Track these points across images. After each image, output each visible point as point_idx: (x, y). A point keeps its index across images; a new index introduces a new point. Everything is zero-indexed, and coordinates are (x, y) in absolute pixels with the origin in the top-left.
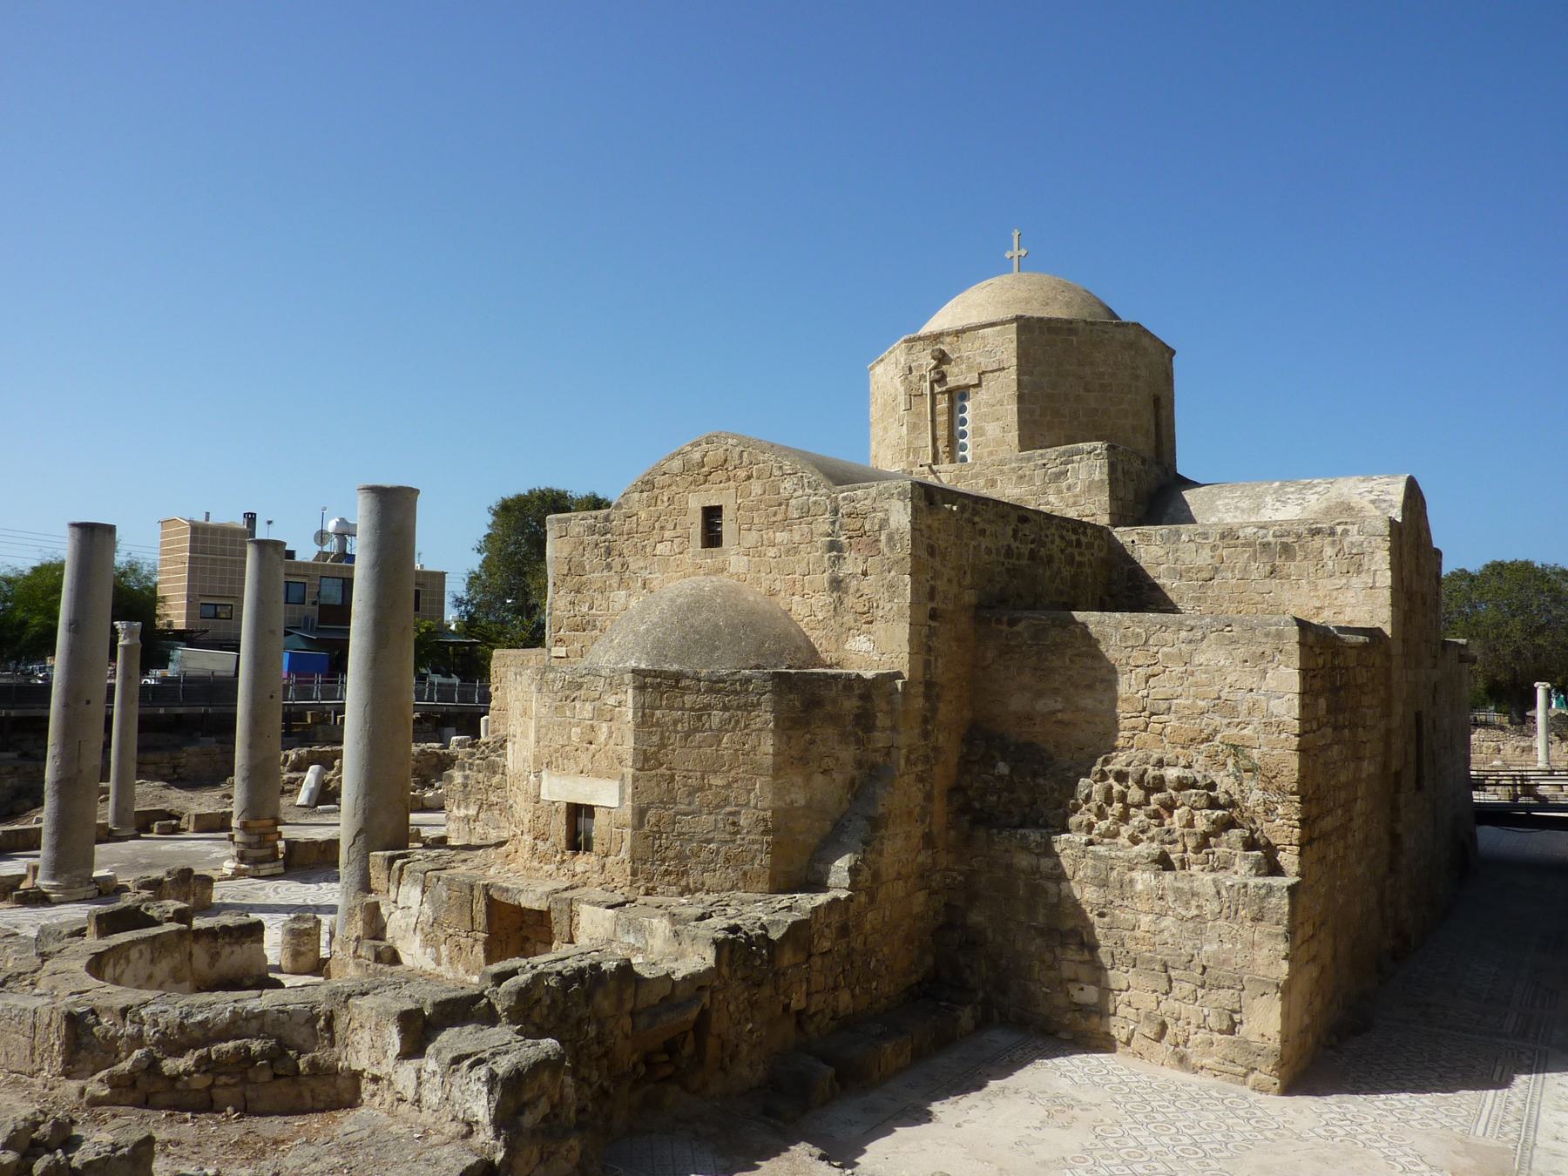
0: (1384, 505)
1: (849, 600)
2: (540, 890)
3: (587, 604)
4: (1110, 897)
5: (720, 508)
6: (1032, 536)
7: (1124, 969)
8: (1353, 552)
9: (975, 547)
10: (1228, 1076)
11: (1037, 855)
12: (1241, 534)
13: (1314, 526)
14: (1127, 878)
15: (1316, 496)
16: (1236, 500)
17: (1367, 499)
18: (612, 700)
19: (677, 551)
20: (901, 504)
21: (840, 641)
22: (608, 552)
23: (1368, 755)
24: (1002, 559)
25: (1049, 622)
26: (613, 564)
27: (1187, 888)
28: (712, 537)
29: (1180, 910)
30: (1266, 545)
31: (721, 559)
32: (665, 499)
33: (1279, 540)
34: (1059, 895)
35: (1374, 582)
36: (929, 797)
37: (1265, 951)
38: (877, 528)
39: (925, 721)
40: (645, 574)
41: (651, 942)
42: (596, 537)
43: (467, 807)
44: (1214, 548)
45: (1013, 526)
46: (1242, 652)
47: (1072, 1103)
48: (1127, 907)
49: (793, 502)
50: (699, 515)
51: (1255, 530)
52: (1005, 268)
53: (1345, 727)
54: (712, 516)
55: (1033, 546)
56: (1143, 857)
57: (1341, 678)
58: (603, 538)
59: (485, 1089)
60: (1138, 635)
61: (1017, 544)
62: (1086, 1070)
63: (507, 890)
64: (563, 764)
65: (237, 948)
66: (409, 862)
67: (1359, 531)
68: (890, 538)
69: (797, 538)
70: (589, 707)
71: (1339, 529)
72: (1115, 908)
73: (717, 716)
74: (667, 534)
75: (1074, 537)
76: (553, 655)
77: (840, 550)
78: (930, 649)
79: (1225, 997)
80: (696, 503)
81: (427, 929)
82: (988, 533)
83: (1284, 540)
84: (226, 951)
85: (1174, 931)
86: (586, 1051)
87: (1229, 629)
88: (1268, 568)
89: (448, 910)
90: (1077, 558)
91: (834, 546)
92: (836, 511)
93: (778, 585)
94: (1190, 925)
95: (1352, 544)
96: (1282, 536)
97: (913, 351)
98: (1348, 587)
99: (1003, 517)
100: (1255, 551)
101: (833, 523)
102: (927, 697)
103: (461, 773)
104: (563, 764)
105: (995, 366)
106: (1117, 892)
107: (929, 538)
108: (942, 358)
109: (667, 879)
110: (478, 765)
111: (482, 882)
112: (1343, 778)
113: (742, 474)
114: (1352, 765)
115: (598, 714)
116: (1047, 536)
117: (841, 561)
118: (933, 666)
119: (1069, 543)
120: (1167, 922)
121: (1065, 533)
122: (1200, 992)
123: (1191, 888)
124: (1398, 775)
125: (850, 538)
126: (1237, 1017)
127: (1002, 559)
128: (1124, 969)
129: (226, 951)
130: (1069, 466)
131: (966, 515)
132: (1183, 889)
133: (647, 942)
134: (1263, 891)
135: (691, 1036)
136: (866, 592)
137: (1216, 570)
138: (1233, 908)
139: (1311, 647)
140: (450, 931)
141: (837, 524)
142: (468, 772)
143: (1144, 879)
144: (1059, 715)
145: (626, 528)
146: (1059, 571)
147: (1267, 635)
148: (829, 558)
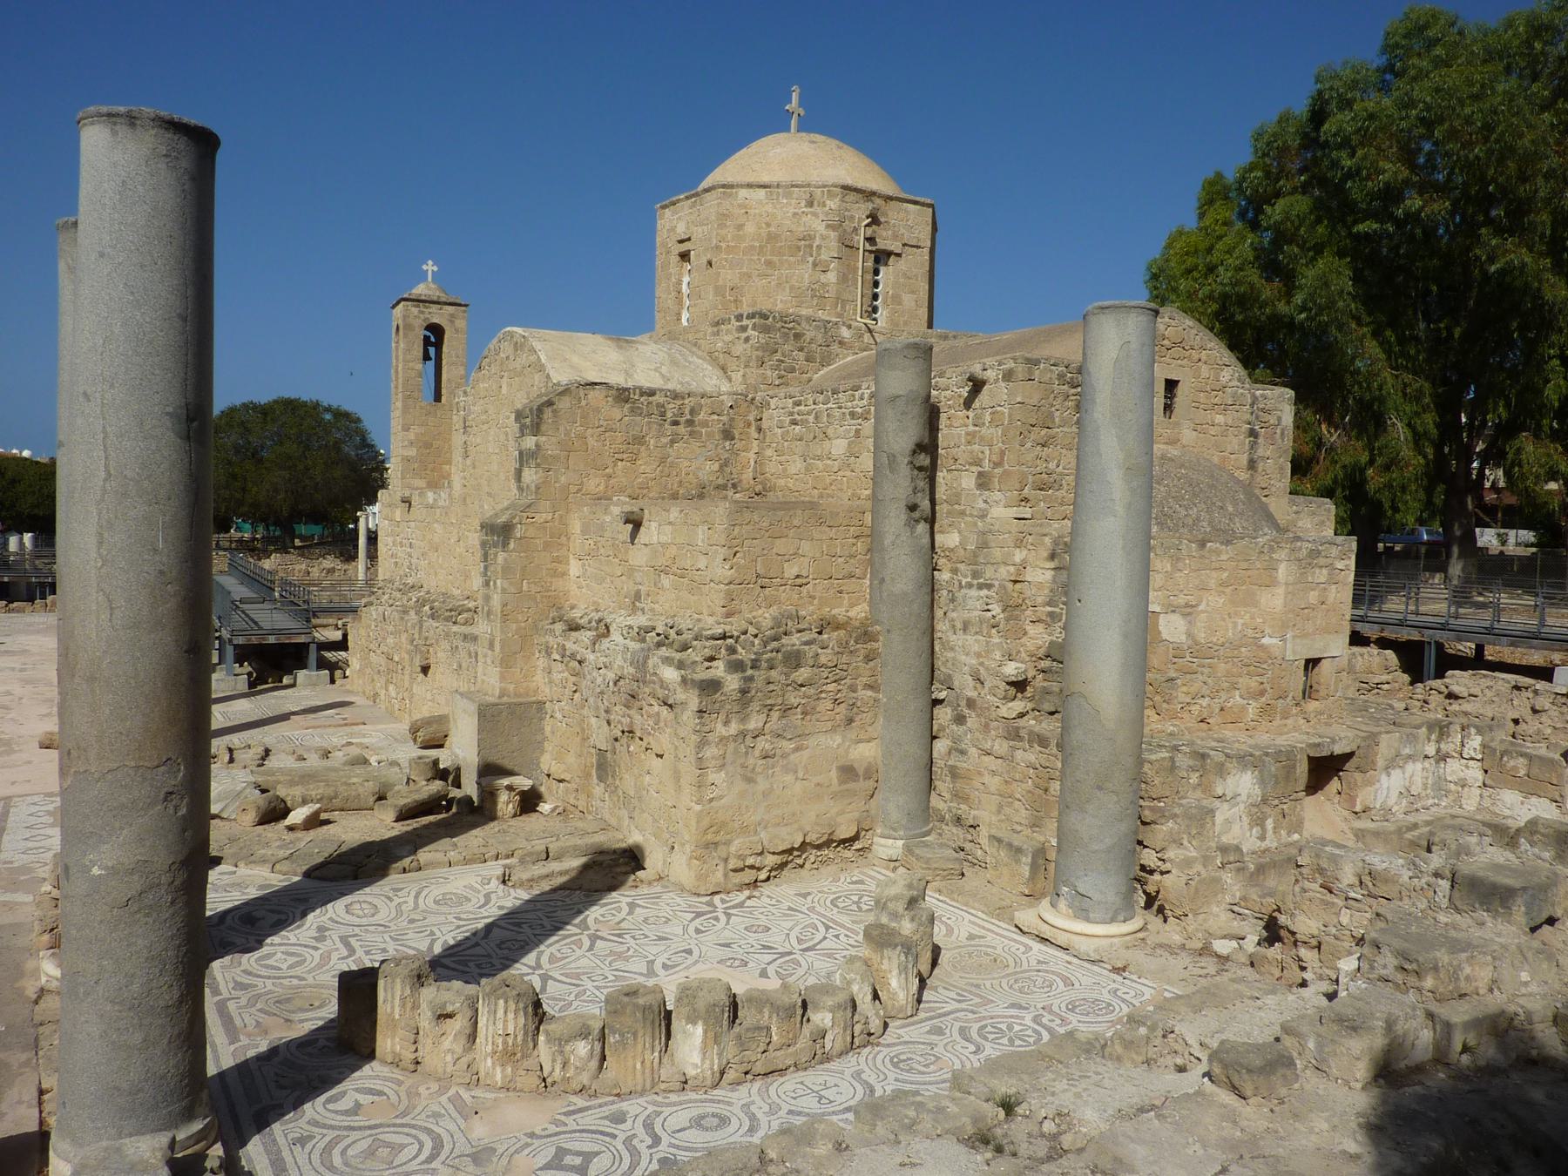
42: (1066, 387)
43: (743, 720)
54: (1171, 385)
70: (1325, 571)
108: (874, 220)
113: (1195, 356)
142: (750, 672)
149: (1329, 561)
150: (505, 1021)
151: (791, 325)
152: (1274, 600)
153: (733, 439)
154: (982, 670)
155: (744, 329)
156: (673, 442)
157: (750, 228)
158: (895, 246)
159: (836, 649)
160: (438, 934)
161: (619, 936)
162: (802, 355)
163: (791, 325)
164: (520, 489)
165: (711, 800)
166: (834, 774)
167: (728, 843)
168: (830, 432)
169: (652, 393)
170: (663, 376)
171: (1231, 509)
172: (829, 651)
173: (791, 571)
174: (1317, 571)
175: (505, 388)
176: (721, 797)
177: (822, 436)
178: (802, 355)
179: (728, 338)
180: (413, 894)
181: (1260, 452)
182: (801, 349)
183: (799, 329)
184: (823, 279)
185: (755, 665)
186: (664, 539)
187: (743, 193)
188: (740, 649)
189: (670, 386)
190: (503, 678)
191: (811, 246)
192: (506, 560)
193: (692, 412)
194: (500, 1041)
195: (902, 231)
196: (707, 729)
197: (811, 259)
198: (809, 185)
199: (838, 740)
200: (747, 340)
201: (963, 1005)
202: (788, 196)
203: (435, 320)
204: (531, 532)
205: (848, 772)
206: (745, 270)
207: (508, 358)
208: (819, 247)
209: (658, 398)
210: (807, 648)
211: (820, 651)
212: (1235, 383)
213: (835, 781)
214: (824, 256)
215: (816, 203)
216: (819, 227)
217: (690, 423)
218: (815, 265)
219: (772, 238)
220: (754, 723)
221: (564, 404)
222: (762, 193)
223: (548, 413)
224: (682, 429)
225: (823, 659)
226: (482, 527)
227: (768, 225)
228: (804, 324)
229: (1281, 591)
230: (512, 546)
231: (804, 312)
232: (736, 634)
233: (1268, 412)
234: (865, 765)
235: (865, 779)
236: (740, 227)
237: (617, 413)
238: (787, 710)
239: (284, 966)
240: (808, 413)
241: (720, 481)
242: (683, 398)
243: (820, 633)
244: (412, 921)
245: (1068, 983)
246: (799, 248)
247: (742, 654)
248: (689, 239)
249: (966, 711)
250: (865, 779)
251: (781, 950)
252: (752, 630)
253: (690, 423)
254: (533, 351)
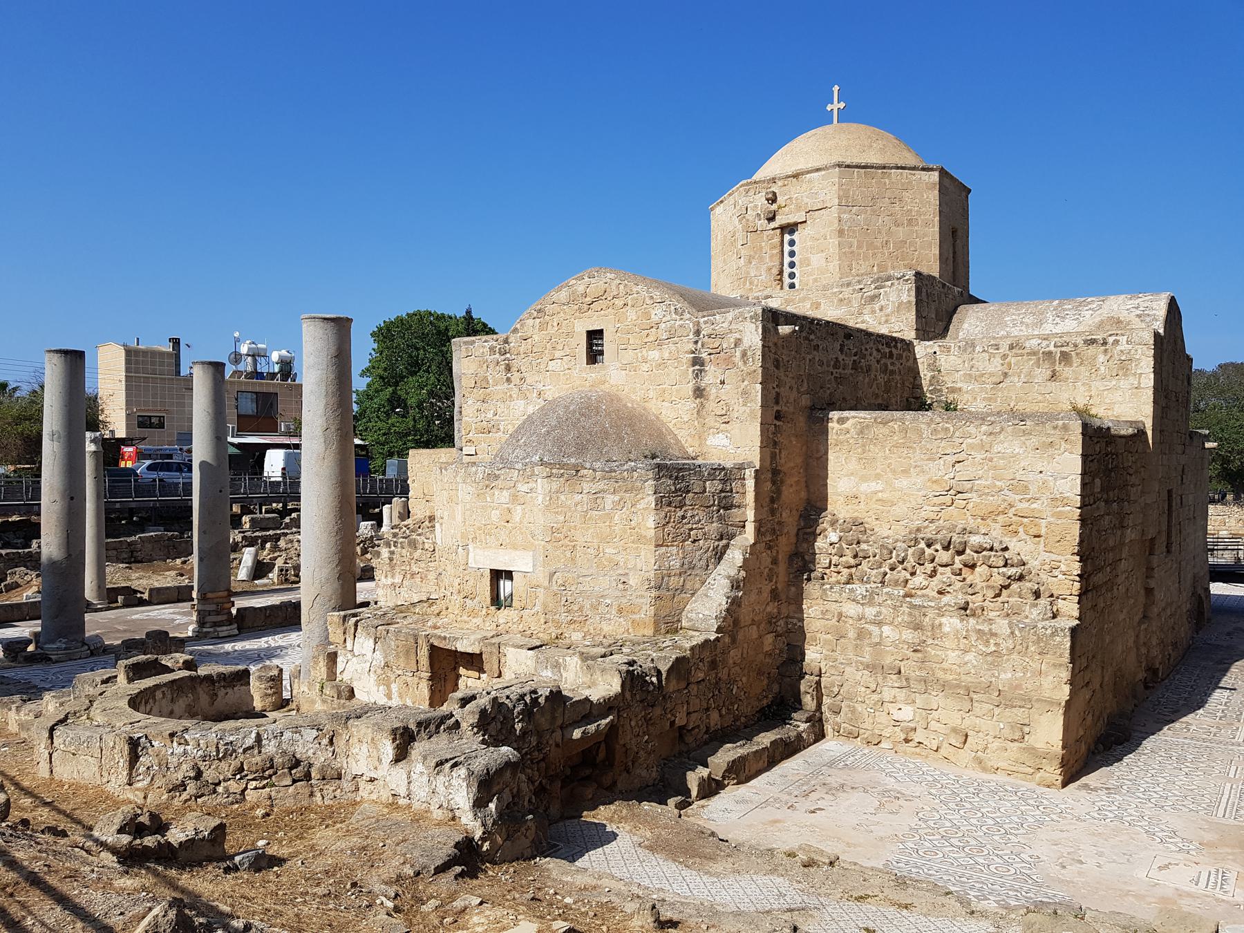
0: (1148, 319)
1: (711, 405)
2: (472, 638)
3: (492, 412)
4: (924, 638)
5: (601, 332)
6: (855, 350)
7: (935, 693)
8: (1123, 358)
9: (810, 360)
10: (1020, 775)
11: (862, 604)
12: (1027, 345)
13: (1089, 338)
14: (937, 622)
15: (1091, 312)
16: (1021, 316)
17: (1134, 314)
18: (525, 488)
19: (566, 367)
20: (753, 325)
21: (701, 437)
22: (508, 368)
23: (1131, 524)
24: (831, 369)
25: (873, 420)
26: (512, 378)
27: (987, 629)
28: (594, 356)
29: (981, 647)
30: (1049, 354)
31: (604, 372)
32: (555, 324)
33: (1059, 349)
34: (881, 636)
35: (1139, 383)
36: (775, 562)
37: (1051, 678)
38: (733, 346)
39: (772, 500)
40: (540, 386)
41: (564, 675)
44: (1005, 356)
45: (840, 342)
46: (1034, 441)
47: (898, 795)
48: (937, 645)
49: (663, 326)
51: (1040, 341)
52: (826, 119)
53: (1115, 501)
55: (855, 358)
56: (950, 605)
57: (1112, 462)
58: (503, 357)
59: (465, 784)
60: (947, 429)
61: (843, 357)
62: (905, 771)
63: (445, 638)
64: (486, 539)
65: (229, 690)
66: (362, 620)
67: (1127, 341)
68: (744, 354)
69: (666, 355)
71: (1111, 340)
72: (927, 646)
73: (610, 499)
75: (887, 350)
76: (464, 453)
77: (702, 364)
78: (775, 443)
79: (1019, 714)
80: (582, 327)
81: (379, 671)
82: (821, 347)
83: (1063, 349)
84: (222, 692)
85: (976, 663)
86: (529, 756)
87: (1024, 423)
88: (1049, 373)
89: (397, 656)
90: (890, 367)
91: (697, 361)
92: (698, 333)
93: (651, 394)
94: (989, 659)
95: (1122, 351)
96: (1062, 346)
97: (750, 194)
98: (1117, 388)
99: (832, 335)
100: (1039, 359)
101: (696, 342)
102: (774, 483)
103: (387, 549)
104: (486, 539)
106: (929, 634)
107: (775, 353)
109: (572, 626)
110: (401, 543)
111: (424, 633)
112: (1111, 543)
113: (620, 303)
114: (1119, 533)
115: (514, 498)
116: (866, 350)
117: (703, 374)
118: (778, 457)
119: (883, 355)
120: (970, 657)
121: (880, 347)
122: (997, 711)
123: (990, 629)
124: (1153, 540)
125: (710, 354)
126: (1026, 729)
127: (831, 369)
128: (935, 693)
129: (222, 692)
130: (882, 291)
131: (804, 334)
132: (983, 631)
133: (561, 675)
134: (1049, 632)
135: (603, 746)
136: (723, 398)
137: (1005, 375)
138: (1025, 645)
139: (1091, 437)
140: (400, 672)
141: (700, 343)
142: (393, 548)
143: (951, 623)
144: (880, 494)
145: (522, 349)
146: (876, 379)
147: (1055, 428)
148: (694, 371)
195: (806, 200)
210: (418, 537)
211: (425, 541)
220: (398, 579)
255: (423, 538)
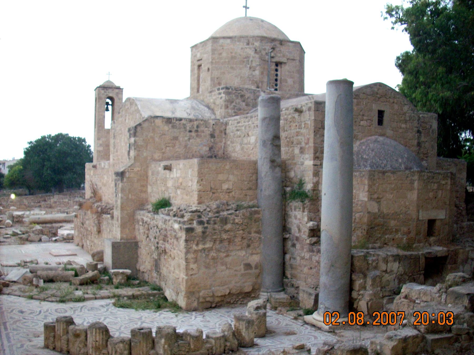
18: (443, 182)
43: (204, 244)
50: (377, 112)
54: (381, 113)
70: (436, 185)
74: (365, 118)
80: (376, 108)
91: (419, 132)
105: (292, 58)
113: (391, 100)
142: (206, 225)
149: (438, 180)
150: (96, 336)
151: (239, 92)
152: (413, 196)
153: (214, 137)
154: (301, 225)
155: (220, 94)
156: (189, 139)
157: (224, 55)
158: (283, 60)
159: (242, 217)
160: (87, 319)
161: (152, 322)
162: (244, 104)
163: (239, 92)
164: (129, 158)
165: (191, 275)
166: (242, 266)
167: (199, 292)
168: (250, 134)
169: (181, 120)
170: (187, 113)
171: (400, 161)
172: (239, 218)
173: (225, 187)
174: (432, 184)
175: (127, 121)
176: (195, 274)
177: (247, 135)
178: (244, 104)
179: (214, 98)
180: (80, 307)
181: (423, 139)
182: (244, 101)
183: (243, 93)
184: (254, 73)
185: (208, 222)
186: (178, 175)
187: (221, 41)
188: (203, 216)
189: (190, 117)
190: (122, 232)
191: (248, 61)
192: (122, 186)
193: (198, 127)
194: (94, 343)
196: (189, 247)
197: (249, 66)
198: (247, 37)
199: (243, 253)
200: (221, 98)
201: (273, 344)
202: (239, 41)
203: (111, 95)
204: (132, 175)
205: (248, 266)
206: (222, 71)
207: (128, 108)
208: (252, 61)
209: (183, 122)
210: (229, 216)
211: (235, 217)
212: (409, 112)
213: (243, 269)
214: (254, 64)
215: (250, 44)
216: (252, 53)
217: (197, 131)
218: (250, 68)
219: (233, 58)
220: (208, 245)
221: (145, 125)
222: (229, 41)
223: (139, 129)
224: (193, 134)
225: (237, 221)
226: (115, 174)
227: (231, 53)
228: (245, 91)
229: (416, 192)
230: (125, 180)
231: (246, 86)
232: (201, 210)
233: (426, 123)
234: (255, 263)
235: (255, 269)
236: (220, 54)
237: (166, 128)
238: (222, 241)
239: (31, 326)
240: (242, 126)
241: (210, 155)
242: (194, 121)
243: (236, 211)
244: (78, 315)
245: (316, 338)
246: (244, 62)
247: (205, 219)
248: (201, 59)
249: (295, 242)
250: (255, 269)
251: (211, 327)
252: (208, 209)
253: (197, 131)
254: (136, 105)
255: (233, 216)
